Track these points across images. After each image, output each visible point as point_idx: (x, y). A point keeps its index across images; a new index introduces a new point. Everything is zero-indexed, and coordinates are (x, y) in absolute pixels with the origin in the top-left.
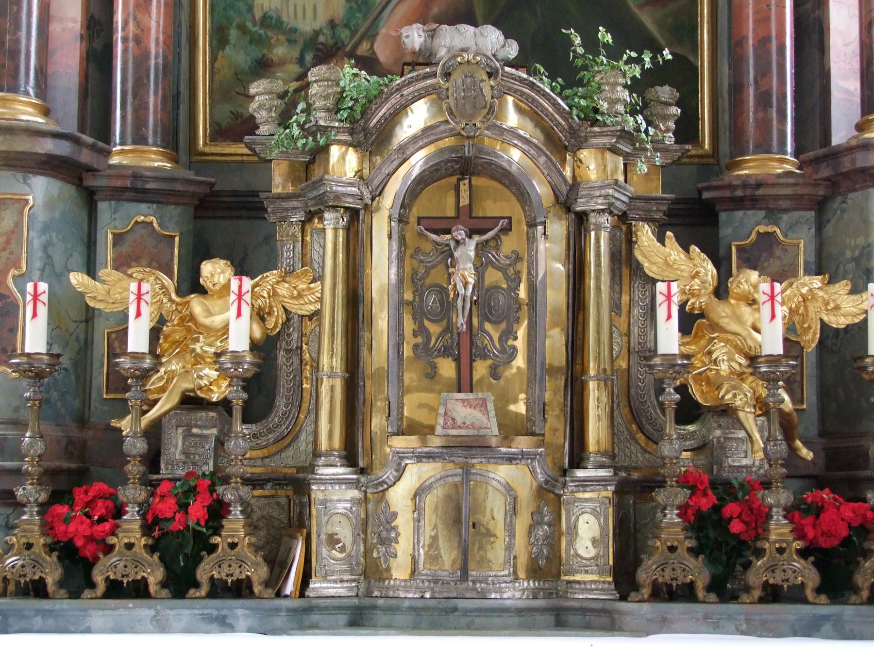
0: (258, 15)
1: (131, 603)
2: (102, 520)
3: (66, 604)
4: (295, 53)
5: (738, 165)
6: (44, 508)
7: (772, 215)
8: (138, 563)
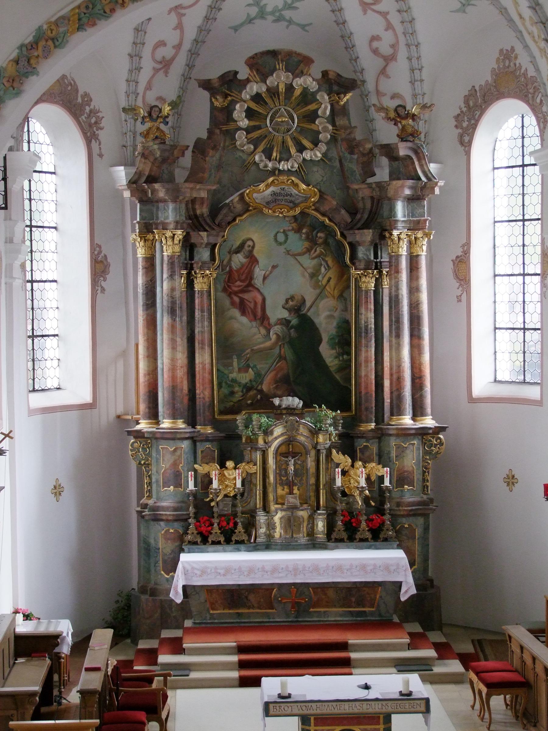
0: (230, 379)
1: (218, 546)
2: (208, 526)
3: (203, 546)
4: (241, 389)
5: (360, 426)
7: (367, 441)
8: (219, 537)
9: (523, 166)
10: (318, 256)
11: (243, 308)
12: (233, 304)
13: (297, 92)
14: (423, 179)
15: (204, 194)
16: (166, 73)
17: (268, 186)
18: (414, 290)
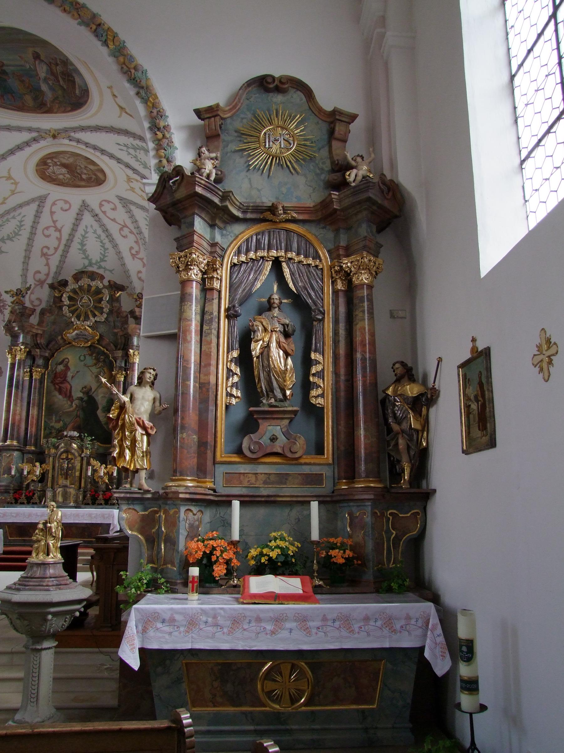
6: (13, 493)
11: (60, 391)
12: (55, 389)
13: (93, 289)
16: (42, 287)
17: (74, 331)
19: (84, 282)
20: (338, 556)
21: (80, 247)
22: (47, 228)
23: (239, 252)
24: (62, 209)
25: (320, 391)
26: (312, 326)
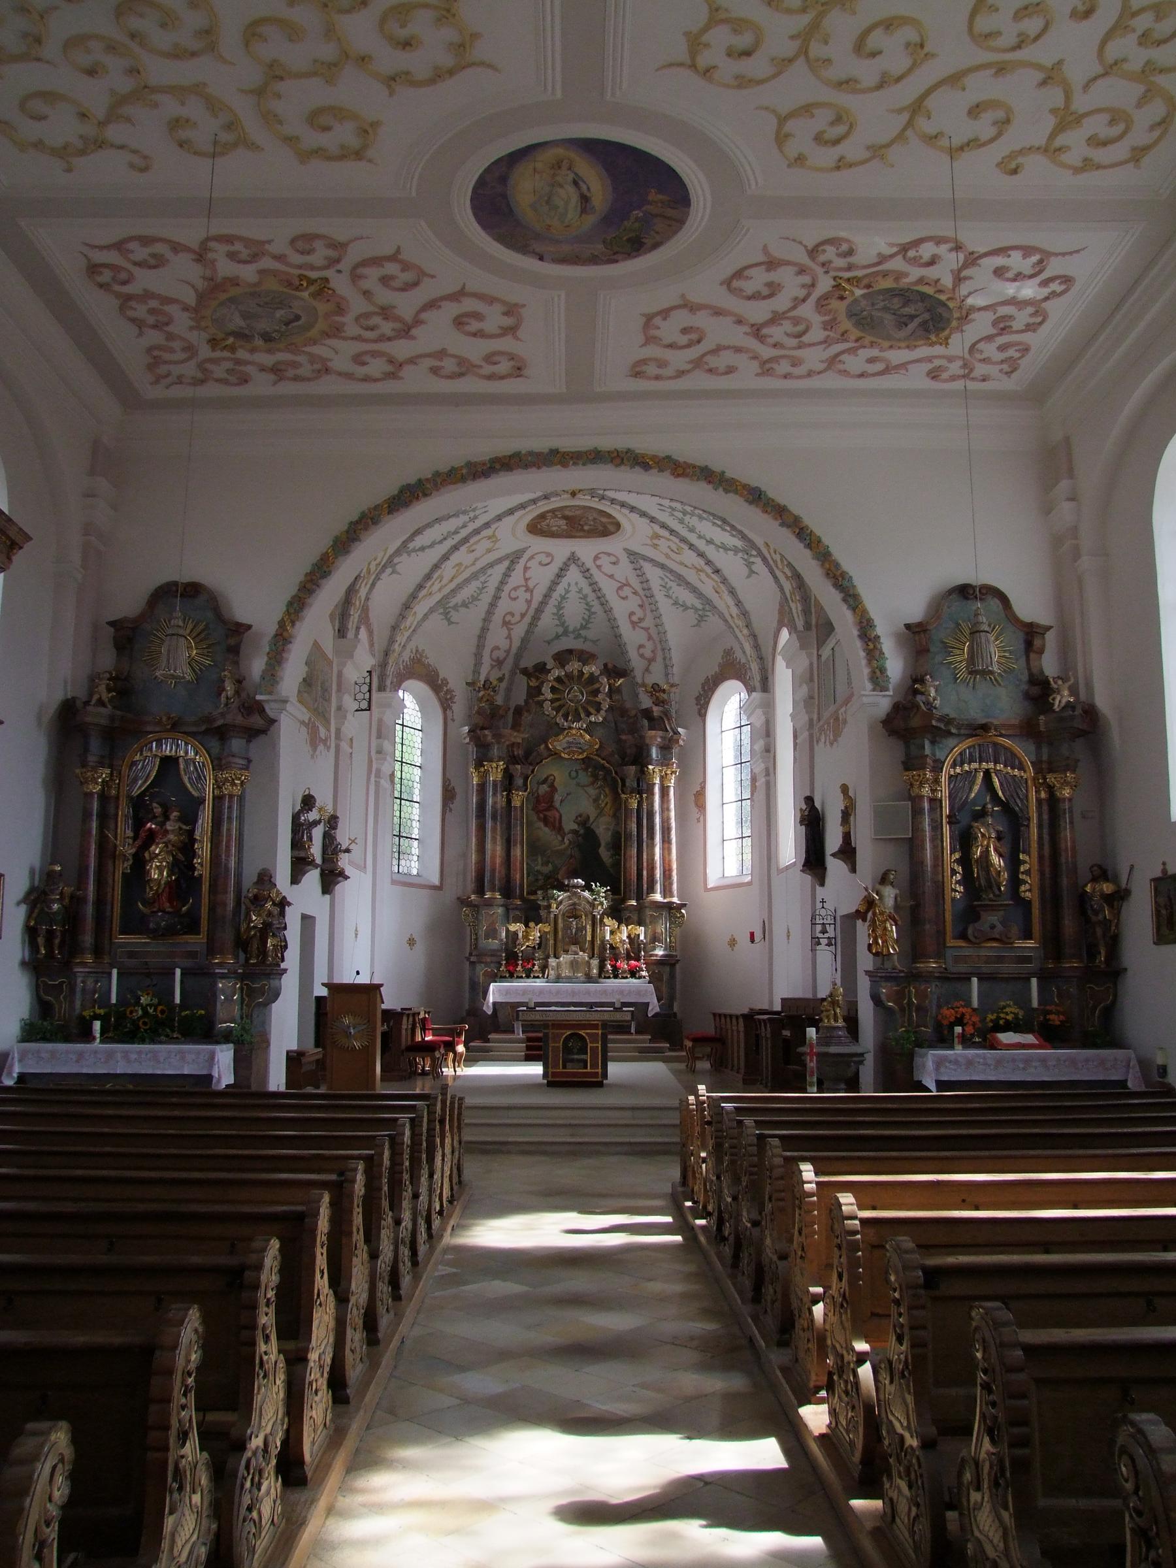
7: (630, 912)
9: (741, 727)
10: (599, 788)
11: (546, 821)
12: (539, 818)
13: (586, 676)
14: (671, 734)
15: (519, 741)
18: (665, 809)
19: (574, 666)
20: (1055, 1019)
21: (555, 611)
22: (515, 589)
23: (954, 766)
24: (540, 564)
25: (1028, 887)
26: (1019, 831)
